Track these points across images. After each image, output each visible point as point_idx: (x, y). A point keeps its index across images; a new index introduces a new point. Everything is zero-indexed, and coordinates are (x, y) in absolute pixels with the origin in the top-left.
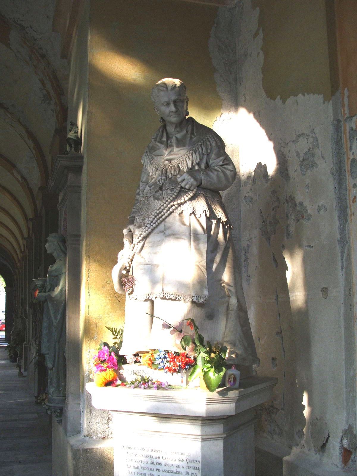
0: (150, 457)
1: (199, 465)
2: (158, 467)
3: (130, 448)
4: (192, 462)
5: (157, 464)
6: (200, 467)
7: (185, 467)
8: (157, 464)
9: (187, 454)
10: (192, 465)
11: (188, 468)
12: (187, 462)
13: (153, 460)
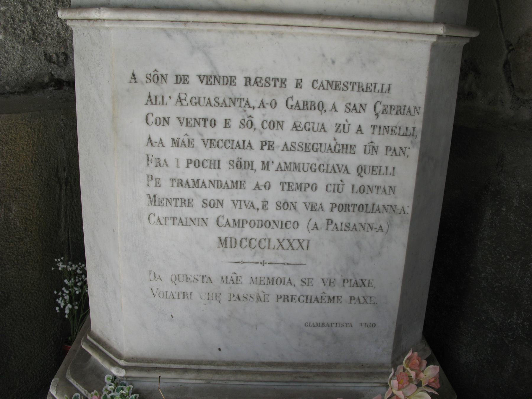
0: (238, 104)
1: (416, 122)
2: (268, 135)
3: (157, 78)
4: (394, 112)
5: (266, 125)
6: (419, 126)
7: (367, 130)
8: (266, 125)
9: (379, 87)
10: (391, 120)
11: (377, 130)
12: (377, 115)
13: (250, 111)
